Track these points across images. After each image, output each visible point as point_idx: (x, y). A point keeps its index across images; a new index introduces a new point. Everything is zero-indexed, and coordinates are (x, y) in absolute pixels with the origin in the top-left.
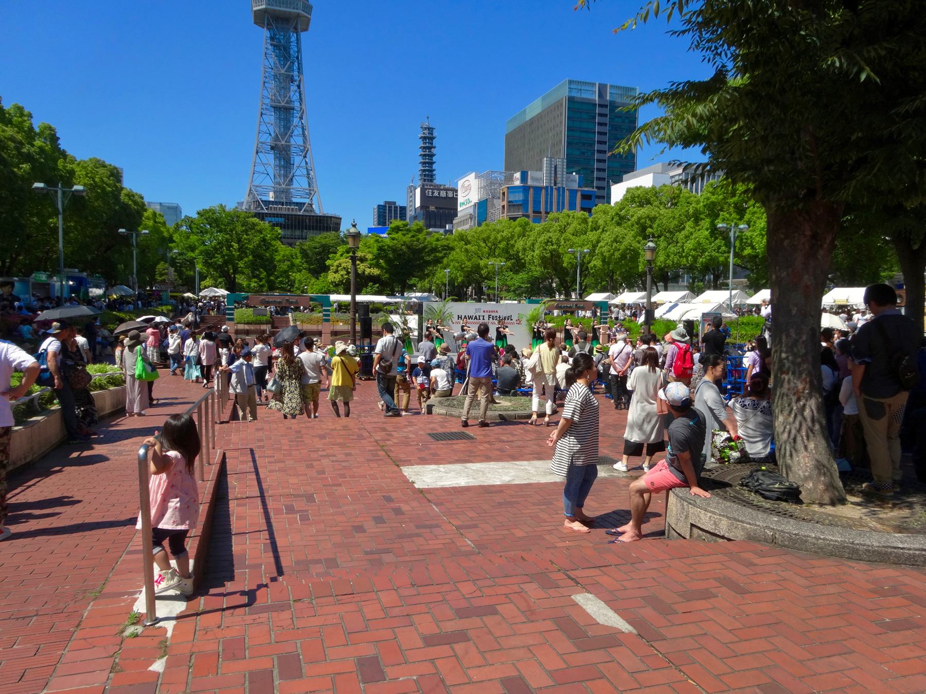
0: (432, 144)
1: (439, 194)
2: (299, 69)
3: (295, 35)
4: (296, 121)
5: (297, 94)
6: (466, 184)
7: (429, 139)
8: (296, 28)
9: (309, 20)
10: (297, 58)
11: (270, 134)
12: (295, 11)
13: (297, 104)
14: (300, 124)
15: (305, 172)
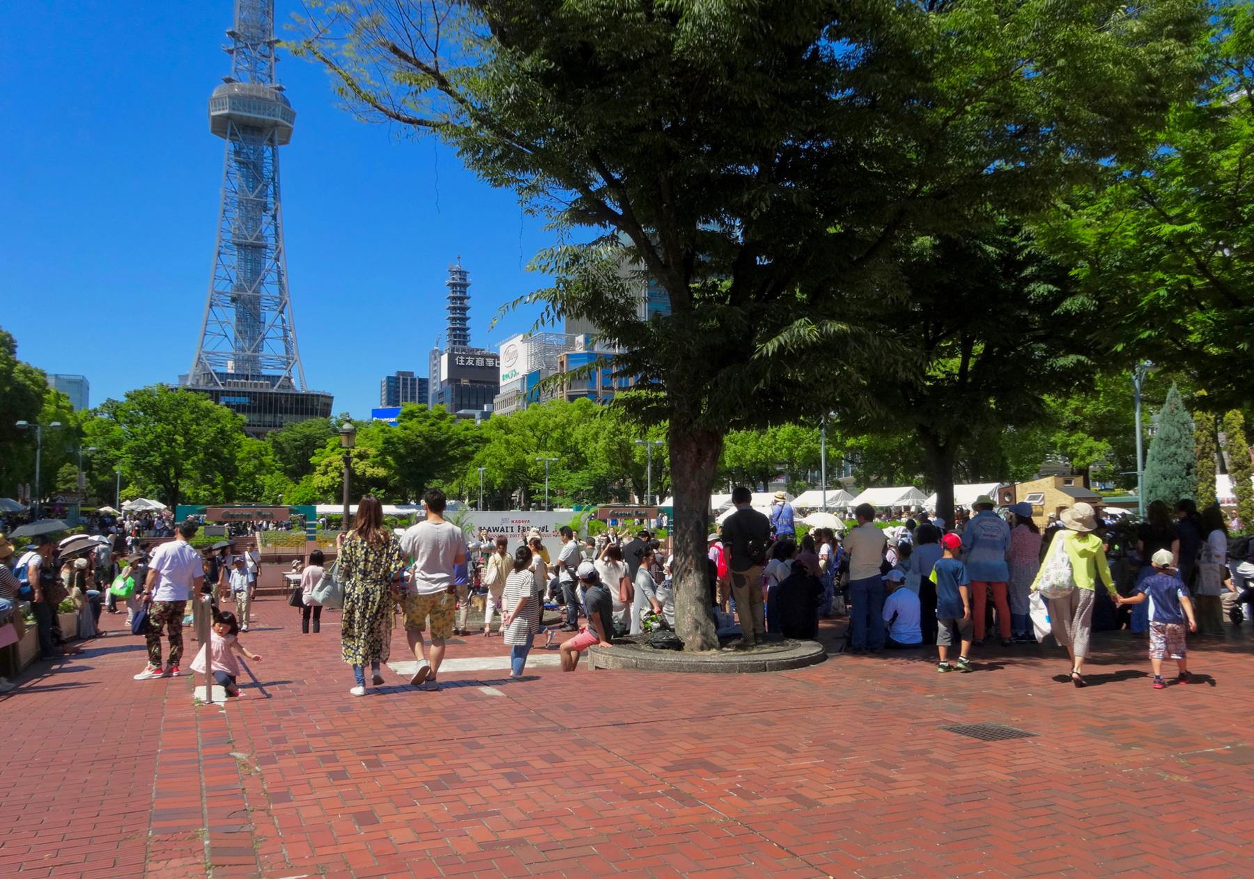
0: (465, 293)
1: (474, 362)
2: (275, 193)
3: (270, 149)
4: (269, 263)
5: (272, 228)
6: (511, 350)
7: (460, 287)
8: (271, 141)
9: (290, 130)
10: (273, 179)
11: (231, 281)
12: (272, 118)
13: (271, 241)
14: (275, 267)
15: (281, 334)
